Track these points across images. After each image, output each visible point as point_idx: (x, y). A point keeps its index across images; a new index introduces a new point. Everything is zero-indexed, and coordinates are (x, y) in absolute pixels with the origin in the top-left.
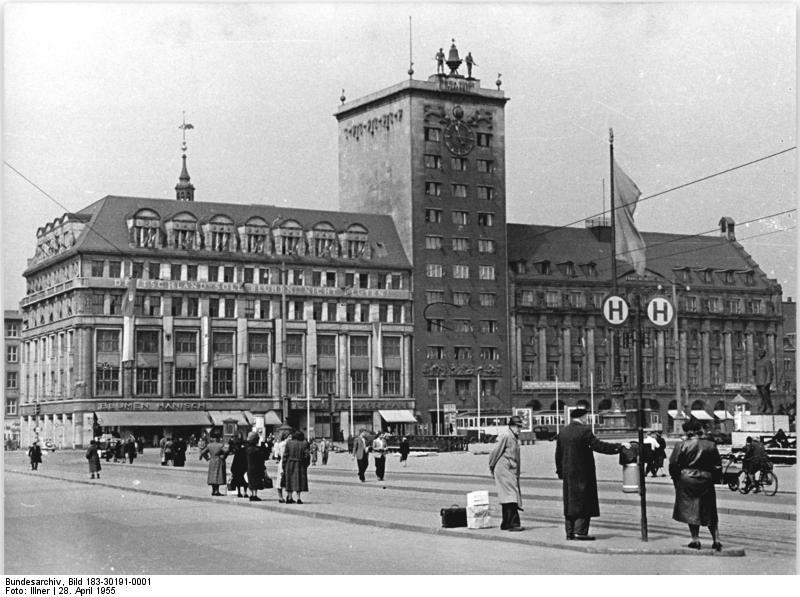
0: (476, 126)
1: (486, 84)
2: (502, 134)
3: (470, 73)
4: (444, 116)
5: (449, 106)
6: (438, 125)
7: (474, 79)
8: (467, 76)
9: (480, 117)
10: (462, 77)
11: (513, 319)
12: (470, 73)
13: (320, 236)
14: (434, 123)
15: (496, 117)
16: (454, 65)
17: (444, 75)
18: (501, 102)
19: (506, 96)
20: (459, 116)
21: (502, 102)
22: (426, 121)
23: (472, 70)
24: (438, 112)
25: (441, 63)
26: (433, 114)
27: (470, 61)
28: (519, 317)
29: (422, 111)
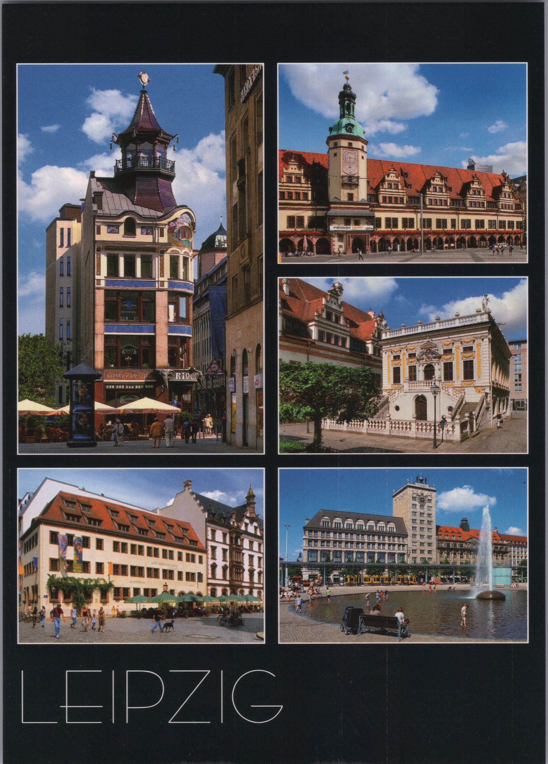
5: (419, 491)
14: (415, 495)
20: (422, 494)
25: (417, 479)
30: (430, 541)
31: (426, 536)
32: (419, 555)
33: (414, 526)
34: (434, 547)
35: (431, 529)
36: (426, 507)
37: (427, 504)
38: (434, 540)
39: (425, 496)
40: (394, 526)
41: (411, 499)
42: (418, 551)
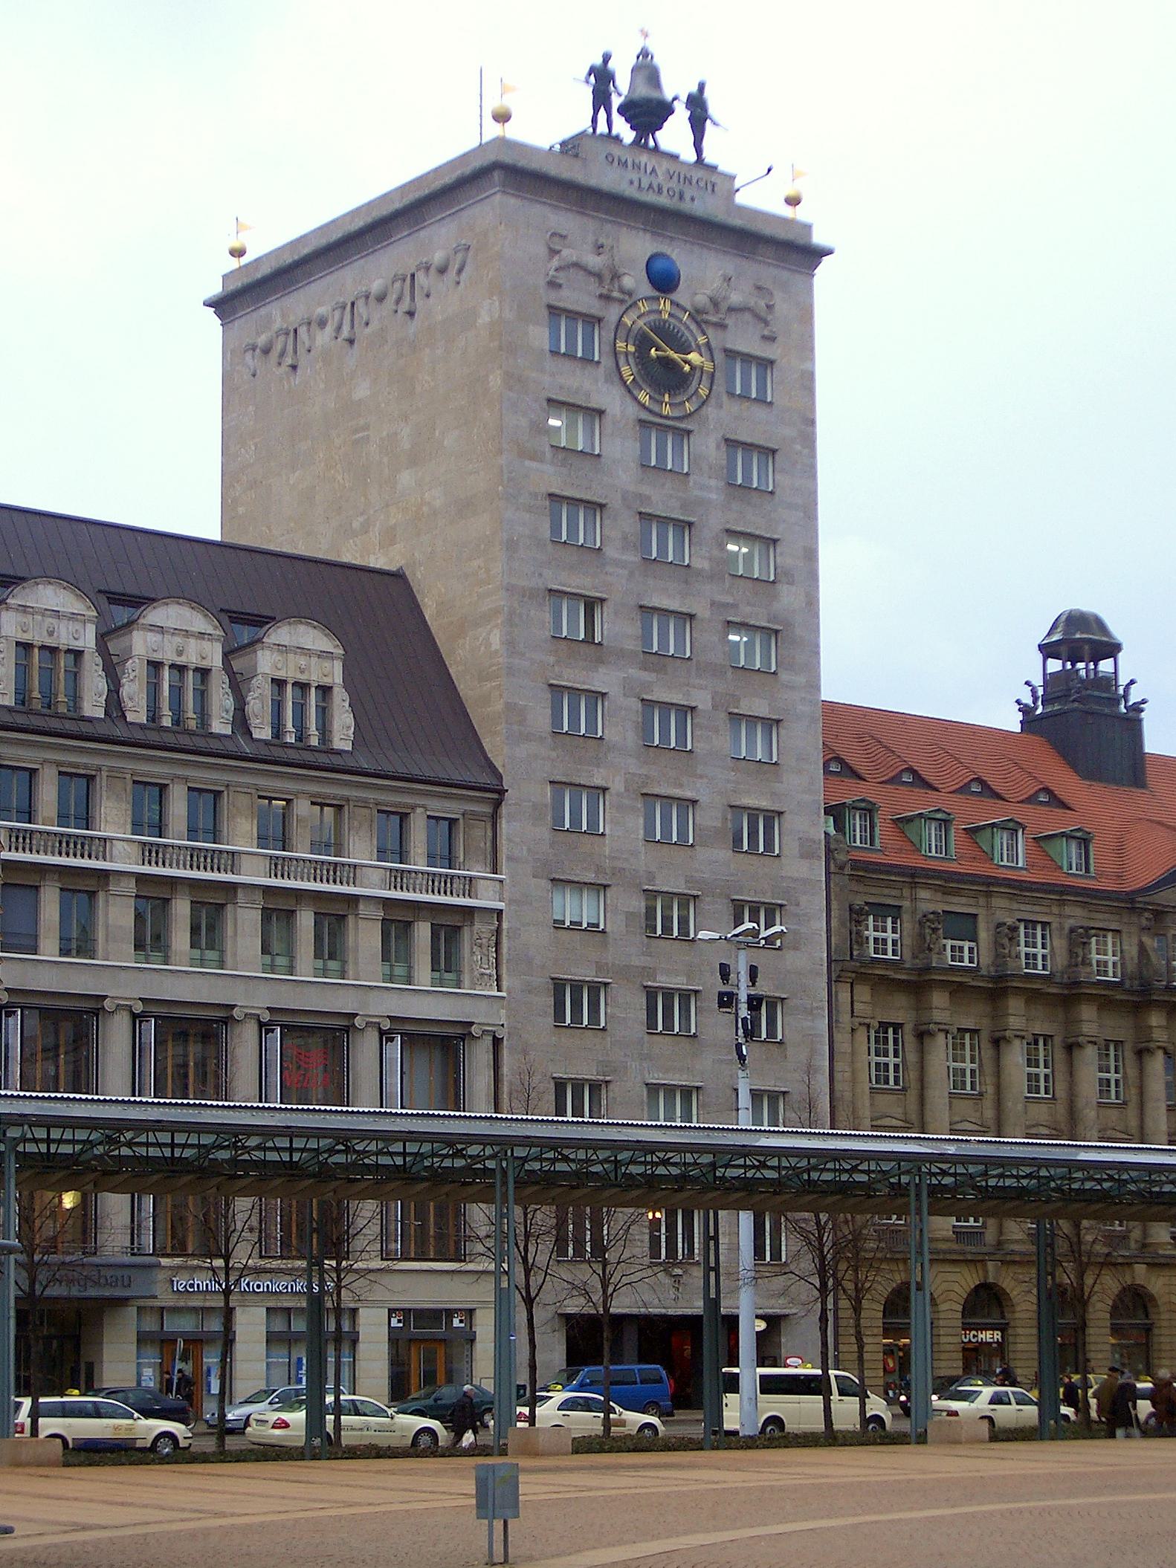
0: (721, 326)
1: (759, 197)
2: (806, 366)
3: (699, 150)
4: (616, 276)
6: (594, 307)
7: (715, 168)
8: (689, 155)
9: (735, 298)
10: (675, 157)
11: (844, 996)
12: (699, 150)
13: (169, 656)
14: (579, 297)
15: (782, 307)
16: (648, 114)
17: (617, 139)
18: (810, 255)
19: (818, 238)
20: (664, 281)
21: (810, 255)
22: (553, 284)
23: (705, 144)
24: (593, 261)
25: (601, 99)
26: (576, 265)
27: (697, 106)
28: (863, 993)
29: (543, 251)
30: (755, 879)
31: (710, 817)
32: (622, 1045)
33: (571, 677)
34: (804, 961)
35: (772, 724)
36: (707, 445)
37: (721, 418)
38: (800, 870)
39: (697, 315)
40: (335, 674)
41: (539, 336)
42: (624, 1008)
